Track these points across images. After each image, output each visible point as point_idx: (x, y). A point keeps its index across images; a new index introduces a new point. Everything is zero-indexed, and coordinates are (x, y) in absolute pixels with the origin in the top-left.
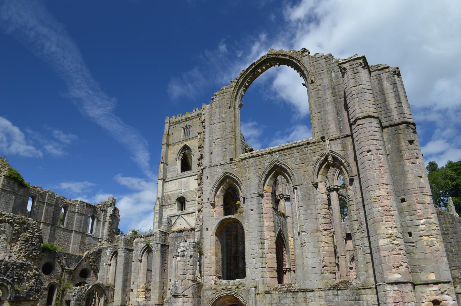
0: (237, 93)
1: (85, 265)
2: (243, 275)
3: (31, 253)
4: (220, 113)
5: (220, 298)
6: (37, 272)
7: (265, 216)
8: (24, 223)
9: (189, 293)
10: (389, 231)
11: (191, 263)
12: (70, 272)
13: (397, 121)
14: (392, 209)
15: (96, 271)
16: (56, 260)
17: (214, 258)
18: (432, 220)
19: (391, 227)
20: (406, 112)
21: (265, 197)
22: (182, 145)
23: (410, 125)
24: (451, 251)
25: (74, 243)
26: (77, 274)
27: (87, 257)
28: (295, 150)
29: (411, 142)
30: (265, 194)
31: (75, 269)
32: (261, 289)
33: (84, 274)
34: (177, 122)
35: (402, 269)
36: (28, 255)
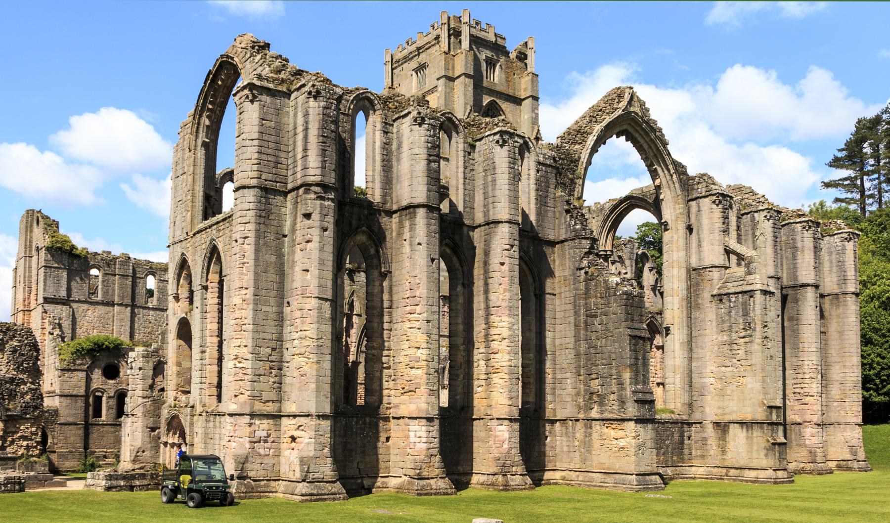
3: (22, 365)
6: (33, 386)
7: (208, 315)
10: (235, 351)
11: (140, 376)
14: (246, 321)
18: (307, 333)
19: (239, 346)
20: (311, 166)
21: (210, 290)
23: (313, 188)
24: (595, 347)
29: (308, 216)
30: (210, 285)
36: (18, 368)
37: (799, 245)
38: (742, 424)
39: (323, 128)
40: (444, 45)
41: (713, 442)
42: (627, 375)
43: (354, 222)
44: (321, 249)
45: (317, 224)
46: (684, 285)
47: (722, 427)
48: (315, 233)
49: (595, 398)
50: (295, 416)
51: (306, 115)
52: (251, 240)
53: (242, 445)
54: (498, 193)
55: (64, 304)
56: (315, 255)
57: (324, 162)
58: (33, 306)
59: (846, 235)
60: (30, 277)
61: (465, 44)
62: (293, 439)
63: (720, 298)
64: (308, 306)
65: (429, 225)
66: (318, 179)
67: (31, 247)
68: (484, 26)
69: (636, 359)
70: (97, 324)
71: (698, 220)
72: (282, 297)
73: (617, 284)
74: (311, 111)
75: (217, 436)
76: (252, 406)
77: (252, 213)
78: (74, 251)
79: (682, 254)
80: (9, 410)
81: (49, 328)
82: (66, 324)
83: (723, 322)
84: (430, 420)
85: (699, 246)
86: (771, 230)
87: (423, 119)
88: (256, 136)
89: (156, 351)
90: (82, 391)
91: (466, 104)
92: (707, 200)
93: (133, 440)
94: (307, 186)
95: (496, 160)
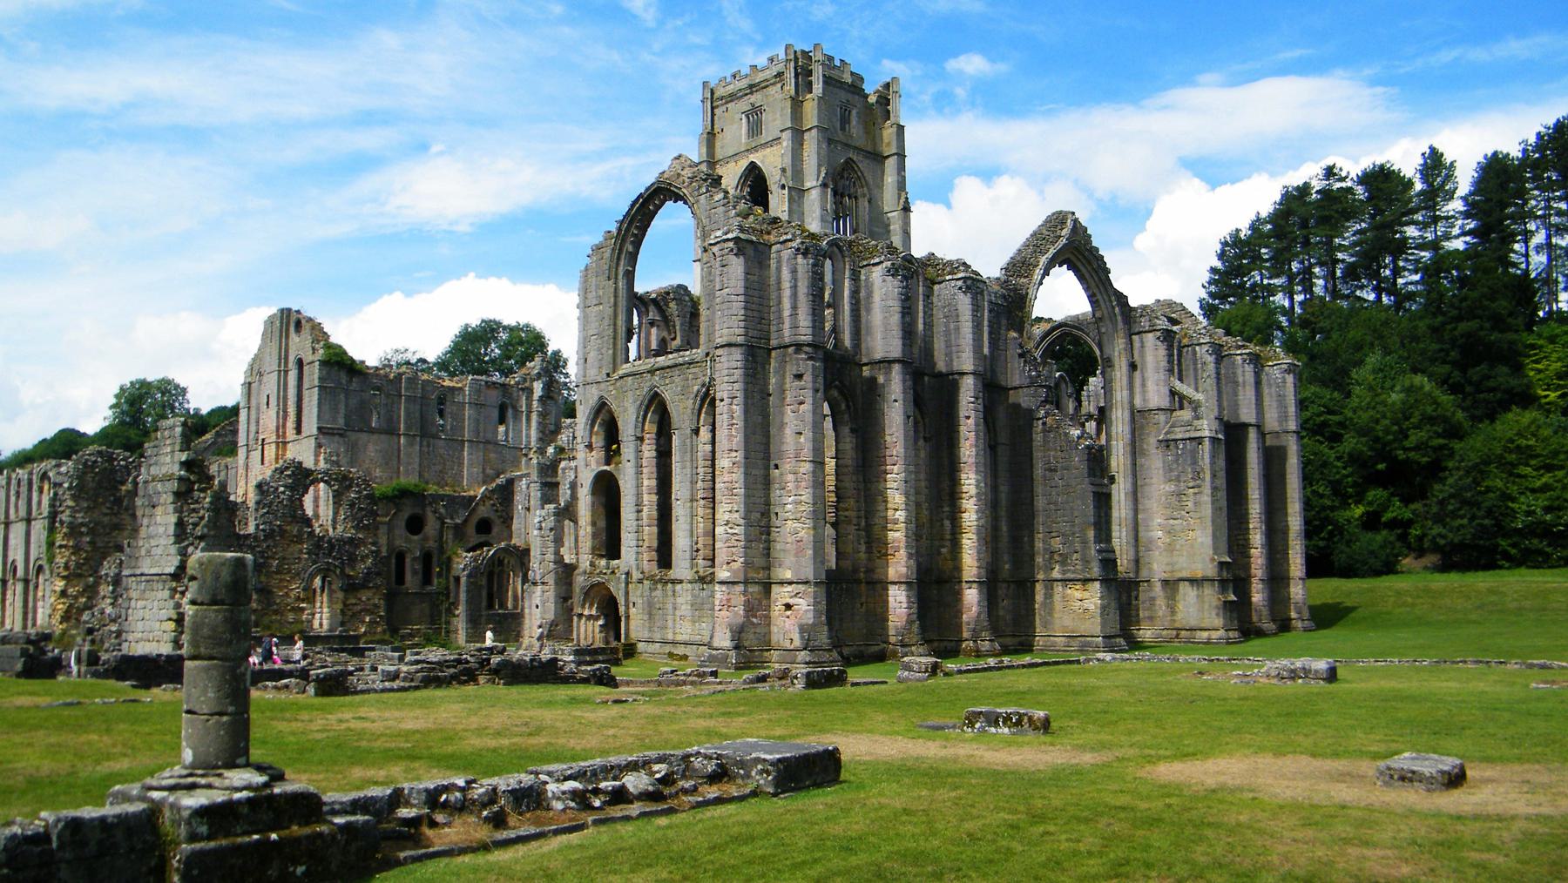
0: (621, 250)
1: (484, 511)
2: (618, 557)
4: (597, 287)
5: (592, 586)
8: (345, 478)
9: (550, 579)
10: (726, 516)
12: (457, 527)
13: (787, 341)
15: (507, 520)
16: (428, 509)
17: (589, 529)
22: (743, 164)
24: (1055, 503)
25: (471, 465)
26: (471, 530)
27: (484, 497)
28: (676, 372)
29: (799, 377)
31: (466, 521)
32: (636, 575)
33: (484, 526)
35: (735, 566)
38: (1193, 581)
41: (1161, 603)
42: (1091, 534)
45: (810, 385)
46: (1127, 429)
47: (1170, 585)
49: (1056, 557)
50: (791, 583)
52: (740, 400)
53: (736, 613)
54: (962, 342)
60: (285, 398)
62: (788, 607)
63: (1167, 443)
65: (904, 381)
66: (809, 338)
71: (1142, 355)
72: (767, 458)
75: (670, 606)
76: (746, 573)
77: (738, 372)
79: (1126, 393)
83: (1171, 470)
85: (1144, 385)
94: (798, 347)
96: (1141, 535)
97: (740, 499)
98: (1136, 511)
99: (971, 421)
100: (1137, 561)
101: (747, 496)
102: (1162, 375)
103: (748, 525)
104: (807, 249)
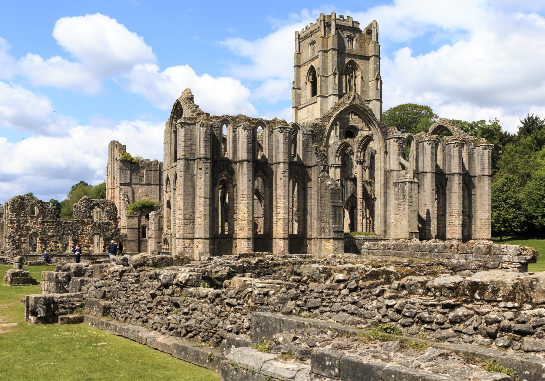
22: (309, 66)
29: (201, 169)
34: (305, 37)
35: (180, 233)
37: (452, 154)
39: (205, 137)
40: (321, 33)
42: (331, 221)
43: (222, 167)
44: (205, 181)
45: (204, 172)
46: (382, 178)
48: (203, 175)
51: (200, 133)
52: (182, 178)
53: (180, 248)
54: (280, 151)
55: (129, 186)
56: (203, 183)
57: (206, 150)
58: (115, 186)
59: (484, 147)
60: (114, 172)
61: (333, 31)
62: (197, 246)
63: (396, 184)
64: (201, 201)
65: (248, 168)
66: (203, 156)
67: (114, 159)
68: (346, 18)
69: (335, 214)
70: (144, 194)
72: (194, 197)
73: (329, 185)
74: (201, 131)
76: (184, 235)
77: (182, 168)
78: (133, 161)
79: (382, 164)
80: (106, 236)
81: (122, 197)
82: (130, 195)
83: (396, 195)
84: (249, 239)
86: (430, 150)
87: (245, 128)
88: (183, 140)
89: (159, 213)
90: (137, 226)
91: (333, 65)
92: (392, 140)
93: (151, 247)
94: (200, 158)
95: (279, 138)
96: (387, 220)
97: (182, 211)
98: (385, 211)
99: (282, 181)
100: (385, 232)
101: (184, 210)
102: (396, 156)
103: (185, 218)
104: (203, 125)
